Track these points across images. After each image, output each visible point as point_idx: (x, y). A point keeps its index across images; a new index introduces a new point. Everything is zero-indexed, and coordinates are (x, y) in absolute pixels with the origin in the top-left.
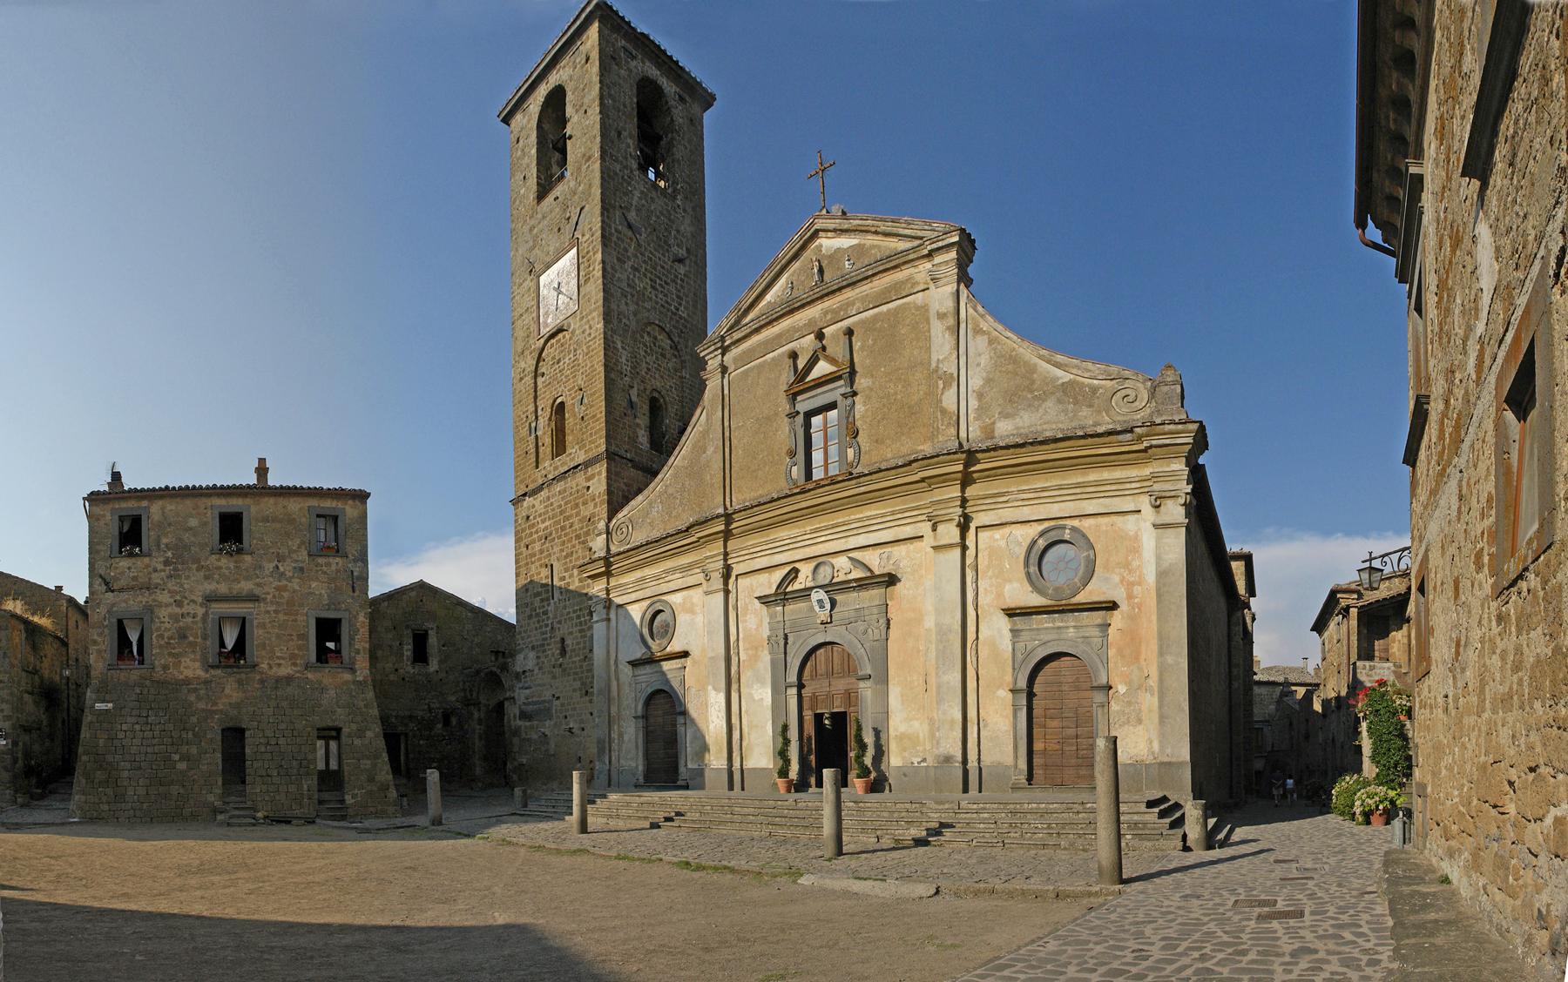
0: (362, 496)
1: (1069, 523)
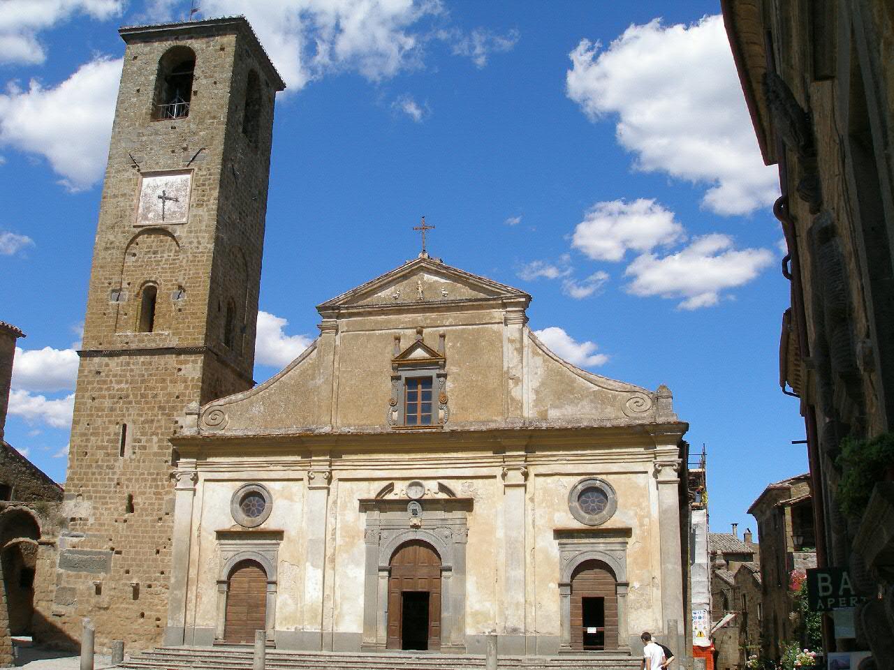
1: (600, 477)
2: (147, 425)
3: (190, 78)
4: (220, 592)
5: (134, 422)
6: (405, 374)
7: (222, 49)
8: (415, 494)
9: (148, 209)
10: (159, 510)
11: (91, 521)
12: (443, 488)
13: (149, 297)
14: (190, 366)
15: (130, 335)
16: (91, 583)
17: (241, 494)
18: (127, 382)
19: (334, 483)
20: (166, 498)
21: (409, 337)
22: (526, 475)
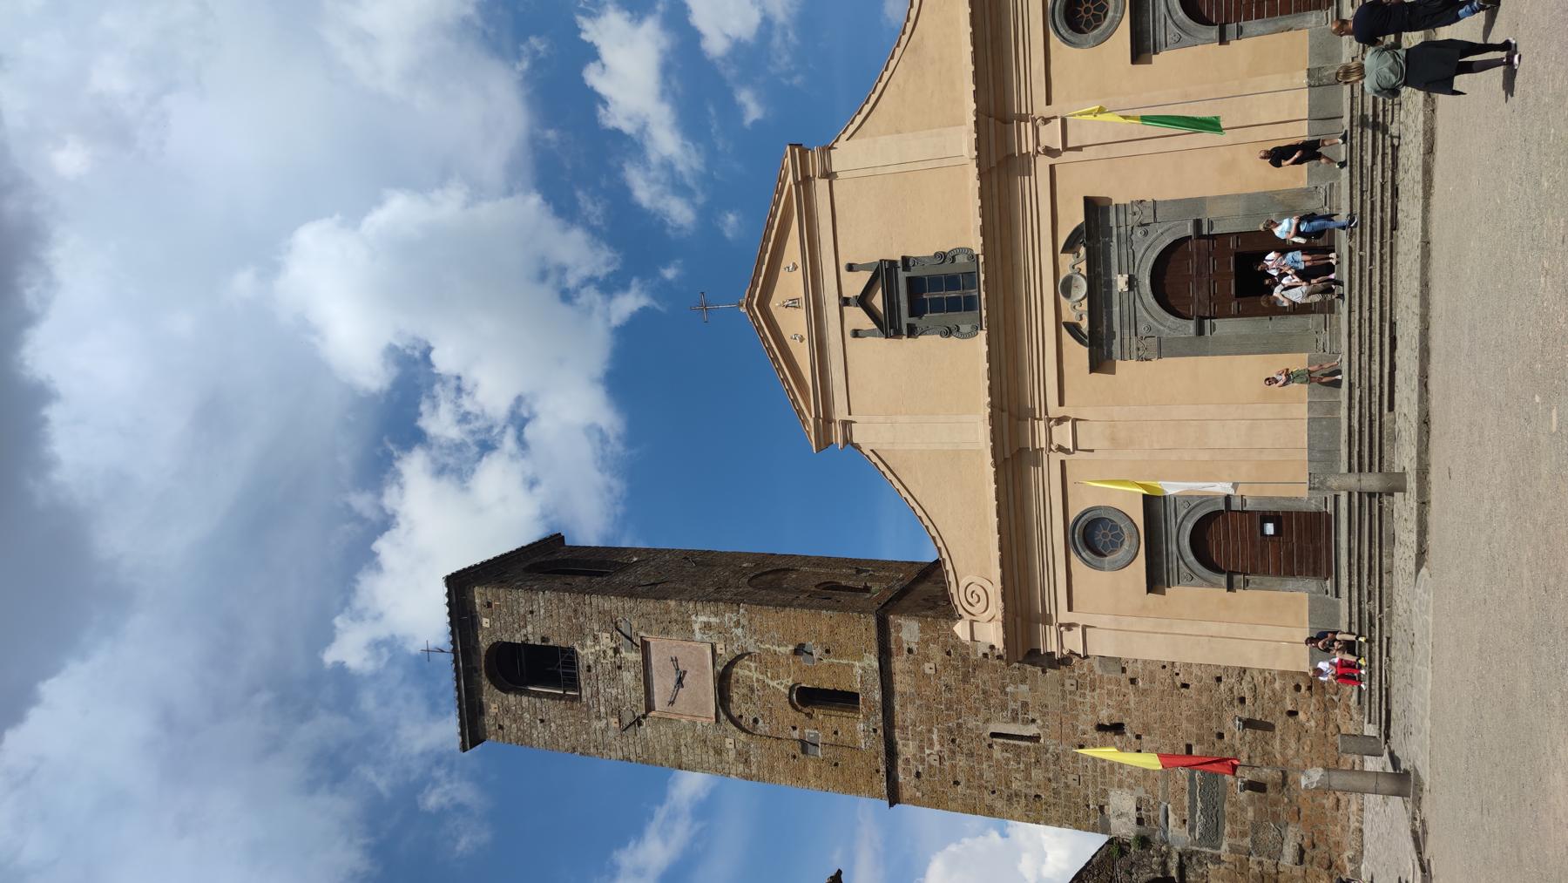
3: (525, 645)
4: (1246, 584)
5: (987, 721)
6: (905, 319)
7: (489, 605)
8: (1081, 288)
10: (1118, 683)
11: (1141, 792)
12: (1070, 246)
13: (808, 698)
14: (904, 635)
15: (861, 729)
16: (1244, 796)
18: (930, 731)
20: (1099, 671)
21: (857, 318)
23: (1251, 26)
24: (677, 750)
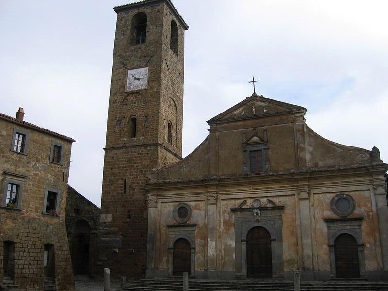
0: (70, 141)
2: (135, 180)
6: (249, 149)
9: (131, 84)
12: (270, 201)
17: (177, 208)
19: (219, 200)
22: (309, 193)
23: (333, 254)
24: (117, 80)
